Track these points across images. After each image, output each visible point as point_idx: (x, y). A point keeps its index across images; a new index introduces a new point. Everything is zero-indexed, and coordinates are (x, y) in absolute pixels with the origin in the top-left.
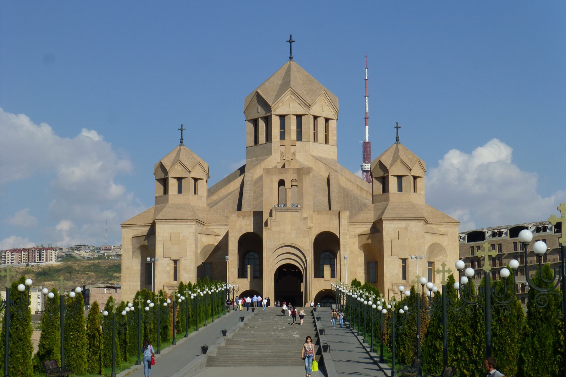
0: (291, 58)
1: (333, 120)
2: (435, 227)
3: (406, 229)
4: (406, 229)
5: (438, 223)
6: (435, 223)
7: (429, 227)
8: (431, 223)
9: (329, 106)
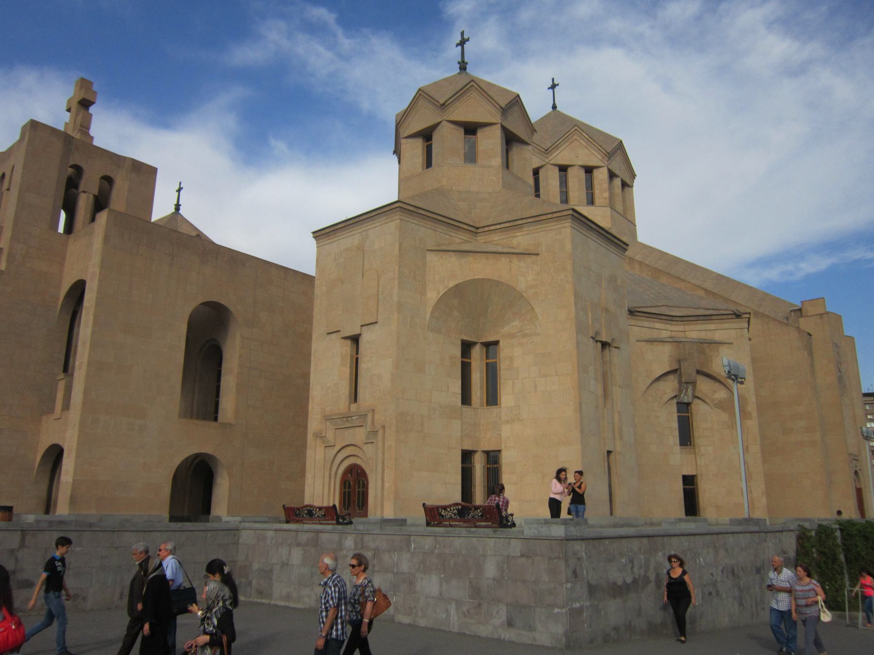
0: (554, 107)
1: (601, 170)
2: (502, 237)
3: (361, 249)
4: (361, 249)
5: (508, 225)
6: (498, 227)
7: (483, 241)
8: (486, 229)
9: (589, 148)
